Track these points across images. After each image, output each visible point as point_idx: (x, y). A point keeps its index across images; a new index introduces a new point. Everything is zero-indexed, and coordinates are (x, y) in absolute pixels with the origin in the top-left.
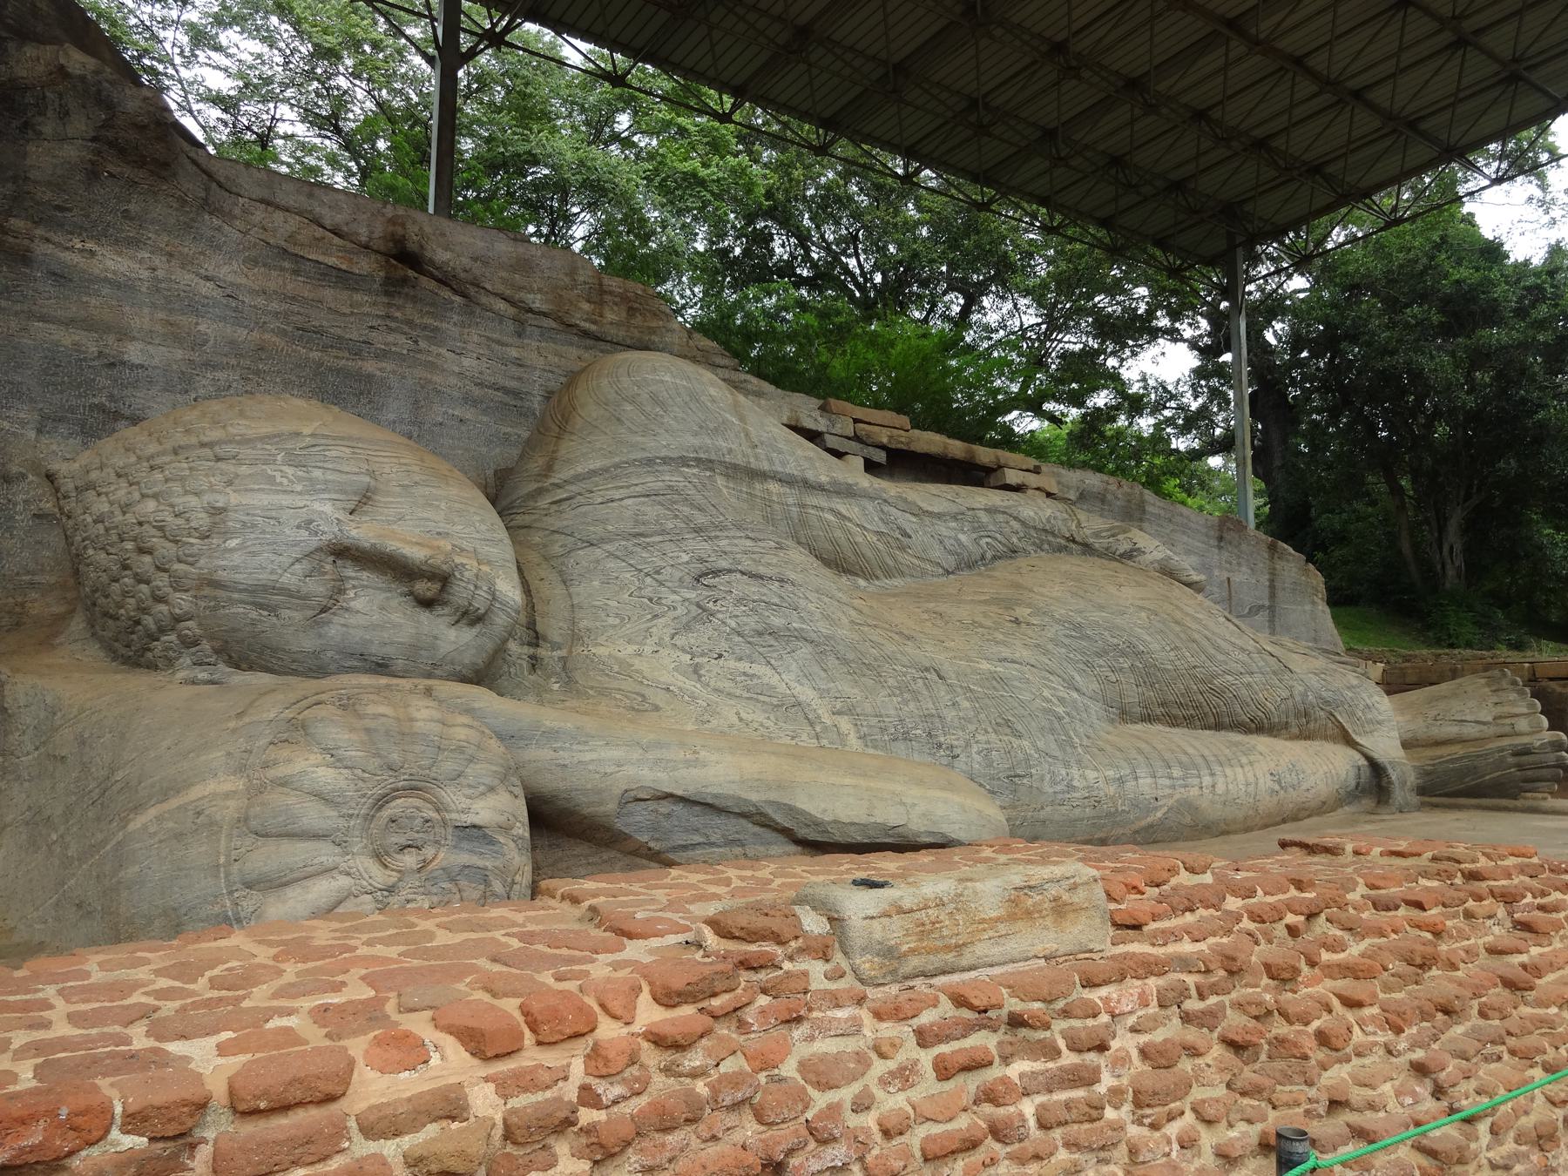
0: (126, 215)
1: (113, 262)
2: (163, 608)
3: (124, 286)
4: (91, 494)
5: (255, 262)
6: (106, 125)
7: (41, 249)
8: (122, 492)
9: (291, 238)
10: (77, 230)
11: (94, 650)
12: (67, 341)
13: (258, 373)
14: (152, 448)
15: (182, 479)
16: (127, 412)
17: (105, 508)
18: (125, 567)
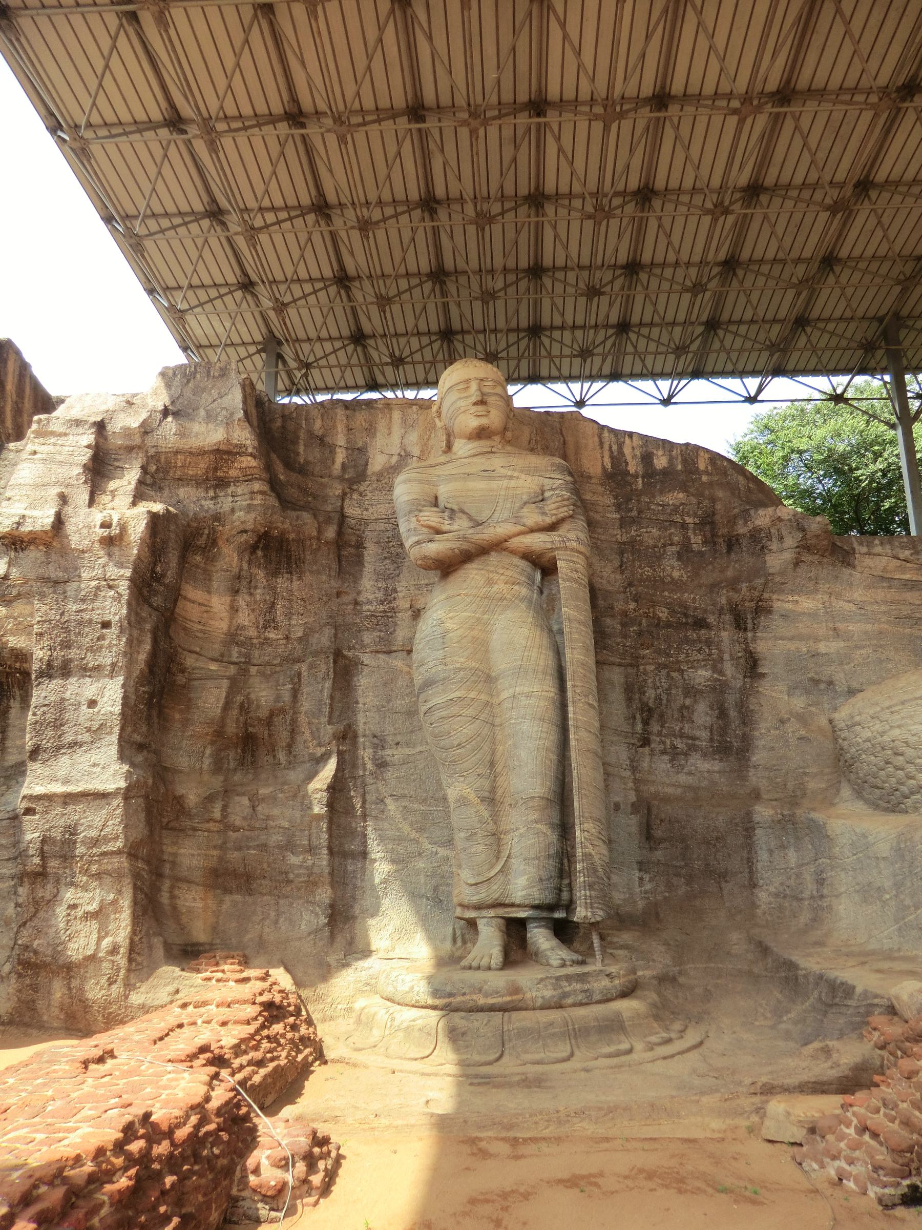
0: (810, 579)
1: (807, 604)
2: (912, 781)
3: (813, 615)
4: (858, 727)
5: (868, 587)
6: (803, 539)
7: (777, 605)
8: (878, 727)
9: (884, 569)
10: (792, 592)
11: (860, 806)
12: (793, 648)
13: (881, 646)
14: (887, 703)
15: (911, 717)
16: (824, 679)
17: (870, 734)
18: (887, 763)
